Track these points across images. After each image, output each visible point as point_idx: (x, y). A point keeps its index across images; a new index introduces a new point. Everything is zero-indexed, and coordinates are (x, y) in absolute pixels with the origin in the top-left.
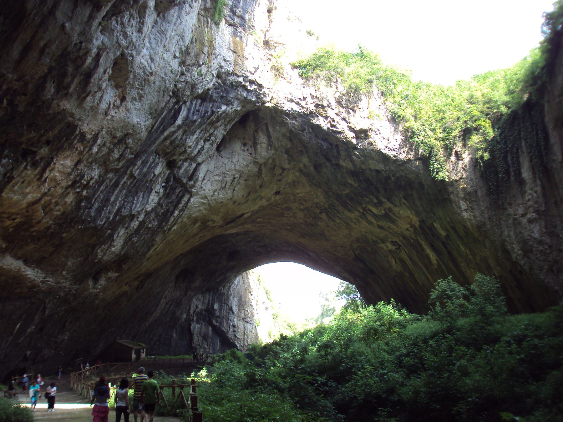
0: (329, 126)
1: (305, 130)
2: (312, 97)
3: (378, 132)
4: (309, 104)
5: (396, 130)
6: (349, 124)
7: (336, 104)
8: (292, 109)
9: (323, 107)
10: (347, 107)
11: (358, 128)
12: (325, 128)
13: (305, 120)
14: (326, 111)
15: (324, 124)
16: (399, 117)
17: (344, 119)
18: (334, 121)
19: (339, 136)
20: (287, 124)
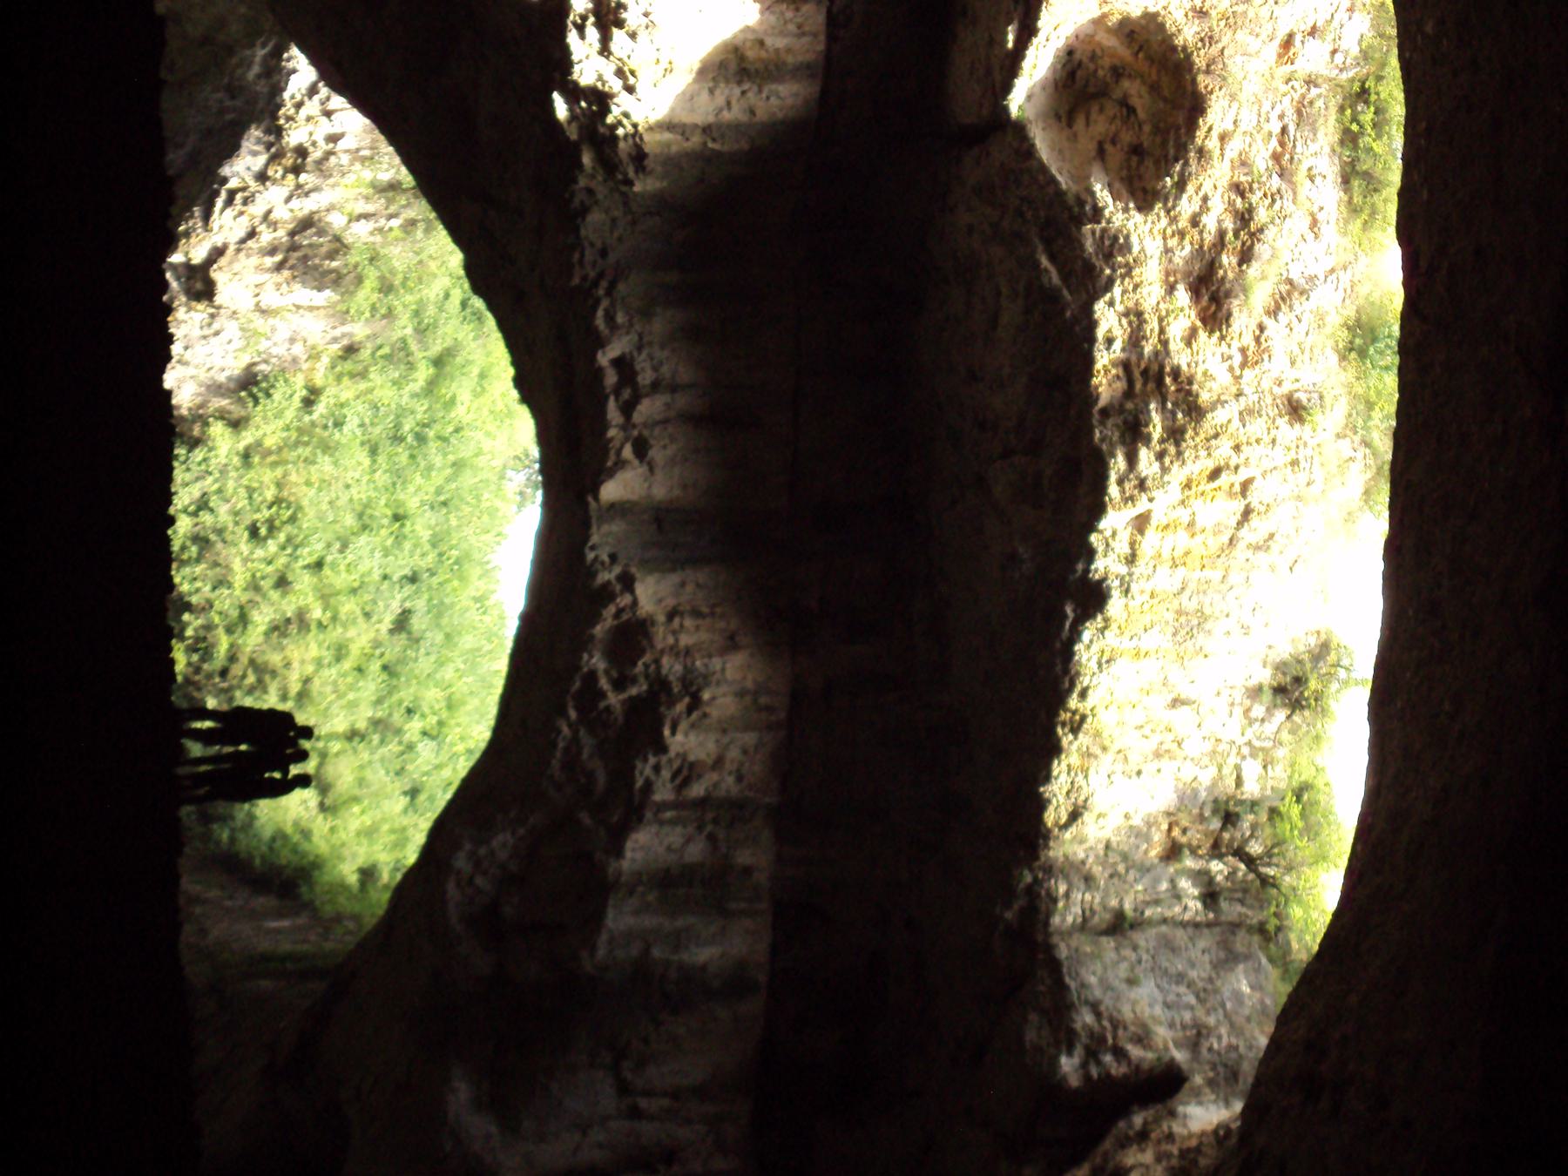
0: (233, 183)
1: (233, 98)
2: (333, 139)
3: (206, 332)
4: (310, 127)
5: (217, 389)
6: (232, 248)
7: (306, 212)
8: (294, 71)
9: (296, 170)
10: (293, 248)
11: (215, 274)
12: (226, 171)
13: (261, 104)
14: (283, 177)
15: (242, 167)
16: (256, 401)
17: (252, 234)
18: (245, 202)
19: (197, 211)
20: (252, 45)
